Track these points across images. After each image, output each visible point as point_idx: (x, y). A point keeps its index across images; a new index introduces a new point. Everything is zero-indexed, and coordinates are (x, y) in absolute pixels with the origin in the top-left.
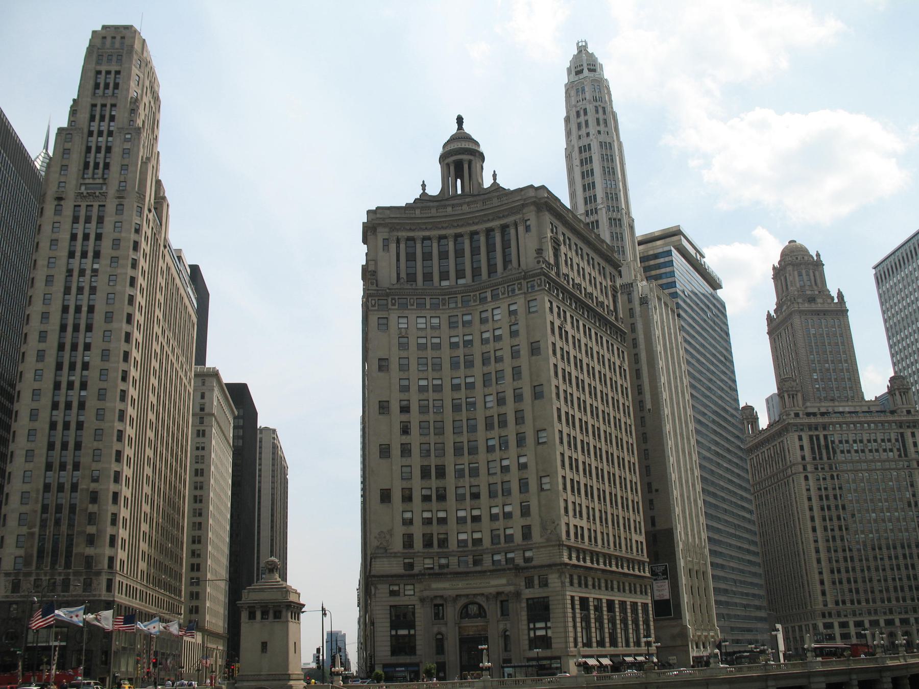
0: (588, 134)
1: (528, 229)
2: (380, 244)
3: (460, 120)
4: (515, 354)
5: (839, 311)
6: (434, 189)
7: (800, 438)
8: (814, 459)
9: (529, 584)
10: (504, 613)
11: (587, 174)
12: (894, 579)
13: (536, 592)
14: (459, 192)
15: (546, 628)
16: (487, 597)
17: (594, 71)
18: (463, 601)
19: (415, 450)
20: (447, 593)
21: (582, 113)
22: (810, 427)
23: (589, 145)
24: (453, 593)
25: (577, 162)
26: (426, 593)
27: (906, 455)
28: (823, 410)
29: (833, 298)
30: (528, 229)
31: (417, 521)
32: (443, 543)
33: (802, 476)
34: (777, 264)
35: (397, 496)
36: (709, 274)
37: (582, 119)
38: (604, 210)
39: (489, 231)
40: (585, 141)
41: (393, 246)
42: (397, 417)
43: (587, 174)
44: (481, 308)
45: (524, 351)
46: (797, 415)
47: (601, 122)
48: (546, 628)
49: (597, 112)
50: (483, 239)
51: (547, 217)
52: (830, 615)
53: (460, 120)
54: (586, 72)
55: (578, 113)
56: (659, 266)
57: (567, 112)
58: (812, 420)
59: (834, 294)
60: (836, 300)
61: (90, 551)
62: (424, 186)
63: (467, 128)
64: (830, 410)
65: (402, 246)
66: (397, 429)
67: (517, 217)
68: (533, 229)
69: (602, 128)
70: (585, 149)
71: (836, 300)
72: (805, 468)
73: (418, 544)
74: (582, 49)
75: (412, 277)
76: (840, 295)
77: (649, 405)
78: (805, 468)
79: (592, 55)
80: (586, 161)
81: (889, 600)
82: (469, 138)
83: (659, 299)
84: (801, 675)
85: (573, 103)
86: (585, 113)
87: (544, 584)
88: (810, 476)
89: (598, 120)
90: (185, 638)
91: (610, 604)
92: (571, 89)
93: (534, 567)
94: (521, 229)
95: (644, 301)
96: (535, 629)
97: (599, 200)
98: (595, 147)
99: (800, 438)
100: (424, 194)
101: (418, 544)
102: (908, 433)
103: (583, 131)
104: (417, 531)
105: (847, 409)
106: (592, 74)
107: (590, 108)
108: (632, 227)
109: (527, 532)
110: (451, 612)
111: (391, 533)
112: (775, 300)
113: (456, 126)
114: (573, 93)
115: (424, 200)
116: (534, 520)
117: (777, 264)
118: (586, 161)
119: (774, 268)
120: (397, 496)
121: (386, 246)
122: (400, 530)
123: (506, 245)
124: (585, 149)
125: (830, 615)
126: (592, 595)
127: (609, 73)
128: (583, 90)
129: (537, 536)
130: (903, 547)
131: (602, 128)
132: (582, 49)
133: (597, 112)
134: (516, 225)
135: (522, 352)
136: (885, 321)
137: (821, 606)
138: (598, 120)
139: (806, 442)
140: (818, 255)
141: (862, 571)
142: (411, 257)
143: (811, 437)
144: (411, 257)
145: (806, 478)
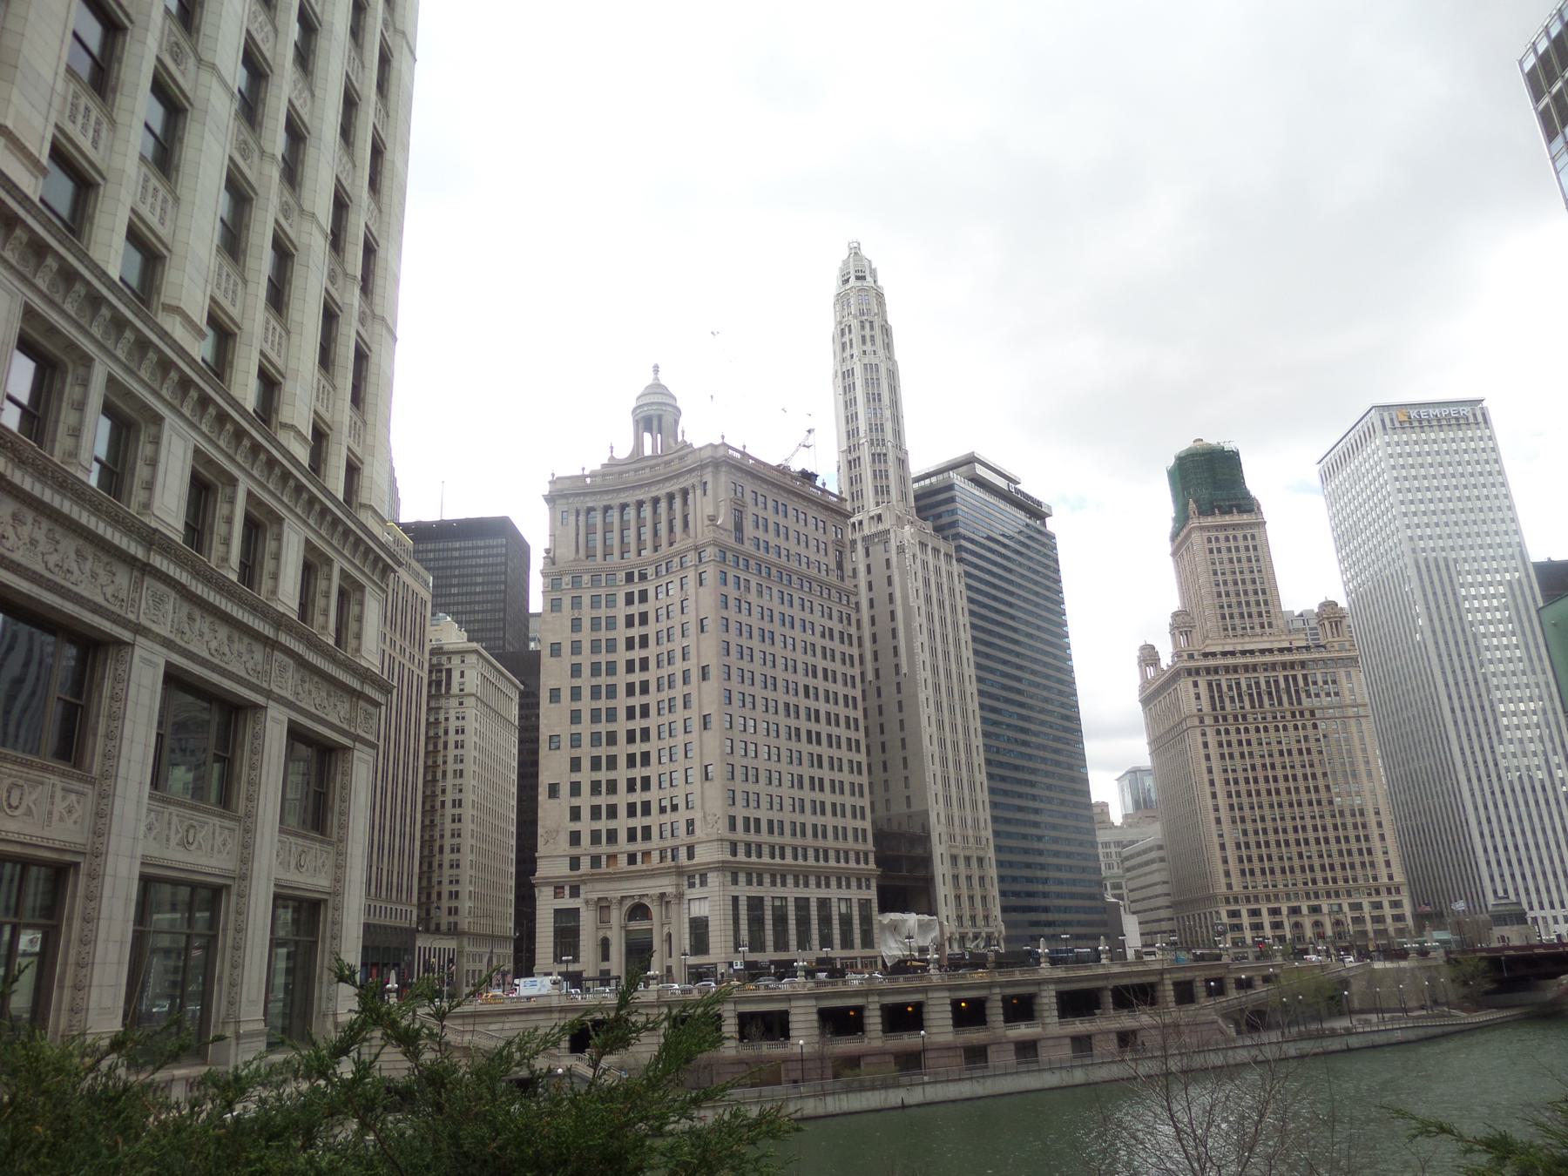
3: (656, 369)
6: (624, 451)
7: (1196, 685)
8: (1214, 709)
11: (850, 403)
12: (1281, 858)
17: (863, 278)
18: (628, 904)
22: (1208, 670)
24: (619, 895)
33: (1198, 731)
37: (846, 338)
39: (671, 497)
41: (572, 519)
46: (1191, 656)
49: (863, 327)
52: (1276, 897)
53: (656, 369)
54: (852, 279)
56: (939, 504)
58: (1211, 662)
63: (664, 380)
65: (582, 518)
69: (868, 347)
72: (1202, 721)
74: (855, 252)
77: (904, 669)
78: (1202, 721)
81: (1335, 881)
83: (923, 545)
84: (916, 990)
88: (1208, 730)
89: (863, 337)
90: (422, 942)
91: (802, 904)
92: (842, 300)
95: (901, 549)
97: (862, 434)
99: (1196, 685)
100: (612, 458)
105: (1276, 645)
106: (859, 283)
107: (855, 324)
108: (902, 463)
110: (616, 916)
118: (848, 389)
125: (1236, 900)
126: (767, 891)
130: (1353, 815)
131: (868, 347)
132: (855, 252)
133: (863, 327)
137: (1224, 889)
138: (863, 337)
139: (1203, 689)
142: (590, 530)
143: (1210, 685)
145: (1204, 734)
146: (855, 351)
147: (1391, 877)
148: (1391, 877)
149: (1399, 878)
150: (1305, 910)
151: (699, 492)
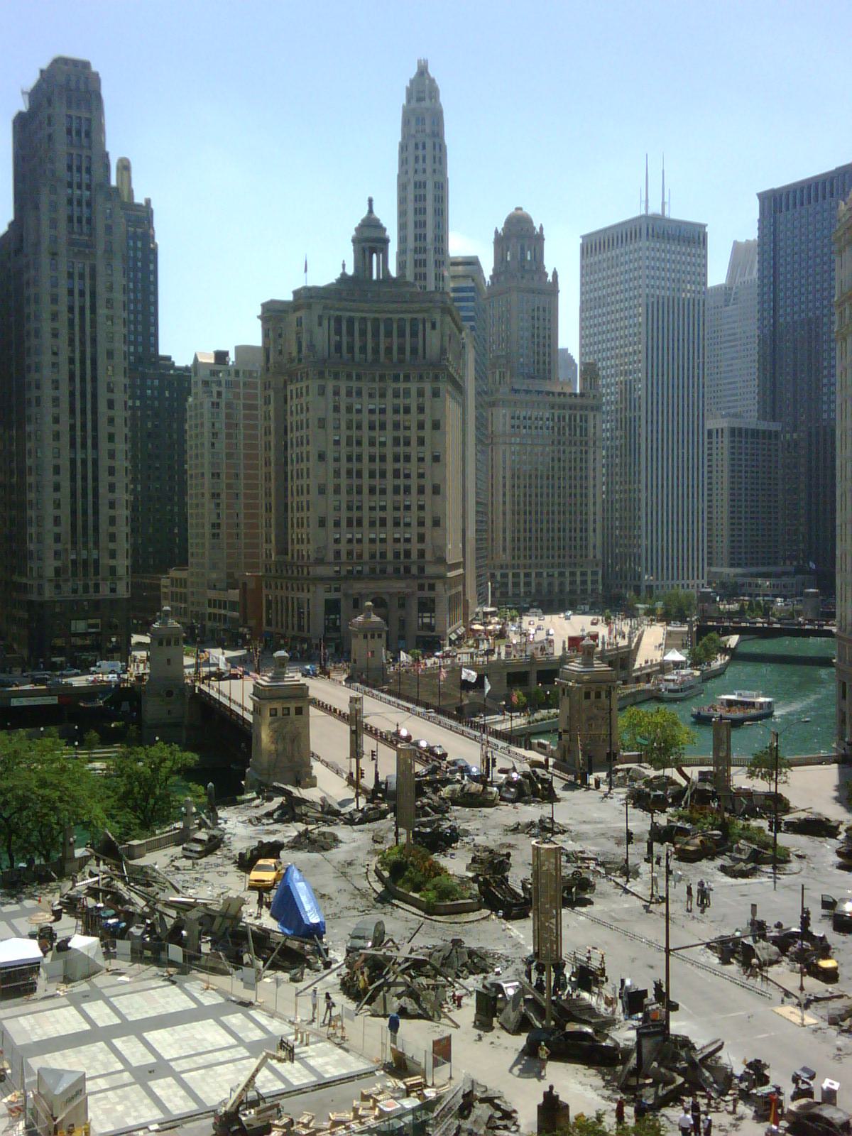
0: (424, 171)
1: (434, 327)
2: (316, 319)
3: (370, 201)
4: (421, 426)
5: (551, 291)
9: (421, 587)
10: (402, 606)
11: (420, 211)
13: (427, 594)
14: (375, 277)
15: (431, 617)
16: (391, 595)
19: (343, 489)
20: (363, 591)
21: (420, 147)
23: (425, 183)
25: (411, 197)
26: (350, 592)
27: (586, 436)
28: (525, 387)
29: (546, 275)
30: (434, 327)
31: (344, 541)
32: (360, 556)
34: (500, 230)
35: (330, 523)
36: (460, 260)
37: (420, 153)
38: (432, 252)
40: (420, 177)
41: (325, 322)
42: (331, 465)
43: (420, 211)
44: (394, 385)
45: (428, 425)
47: (437, 159)
48: (431, 617)
49: (434, 148)
50: (395, 326)
51: (448, 319)
53: (370, 201)
55: (417, 146)
57: (404, 137)
59: (549, 271)
60: (550, 278)
61: (112, 562)
62: (344, 266)
63: (378, 213)
64: (531, 388)
65: (332, 323)
66: (331, 474)
67: (426, 315)
68: (438, 325)
70: (420, 185)
71: (550, 278)
73: (344, 557)
74: (423, 71)
75: (338, 347)
76: (555, 275)
79: (432, 81)
80: (420, 198)
82: (377, 221)
85: (413, 131)
86: (424, 147)
87: (432, 587)
93: (427, 577)
94: (428, 325)
96: (422, 617)
98: (430, 185)
100: (344, 274)
101: (344, 557)
102: (591, 415)
103: (420, 166)
104: (343, 547)
107: (429, 146)
109: (422, 554)
111: (325, 547)
112: (399, 139)
113: (367, 208)
114: (413, 122)
115: (344, 278)
116: (427, 547)
117: (500, 230)
118: (420, 198)
119: (496, 231)
120: (330, 523)
121: (320, 324)
122: (332, 547)
123: (414, 334)
124: (420, 185)
127: (445, 100)
128: (423, 120)
129: (428, 557)
132: (423, 71)
134: (424, 321)
135: (426, 427)
136: (582, 294)
138: (434, 158)
140: (541, 228)
141: (536, 531)
142: (338, 332)
144: (338, 332)
146: (429, 171)
147: (595, 557)
148: (595, 557)
149: (599, 556)
150: (545, 575)
151: (428, 325)
